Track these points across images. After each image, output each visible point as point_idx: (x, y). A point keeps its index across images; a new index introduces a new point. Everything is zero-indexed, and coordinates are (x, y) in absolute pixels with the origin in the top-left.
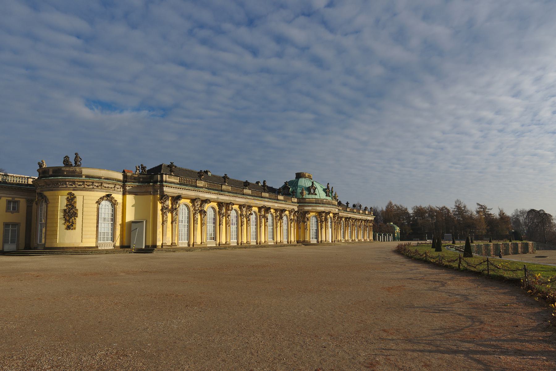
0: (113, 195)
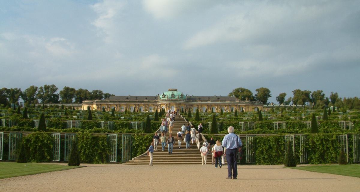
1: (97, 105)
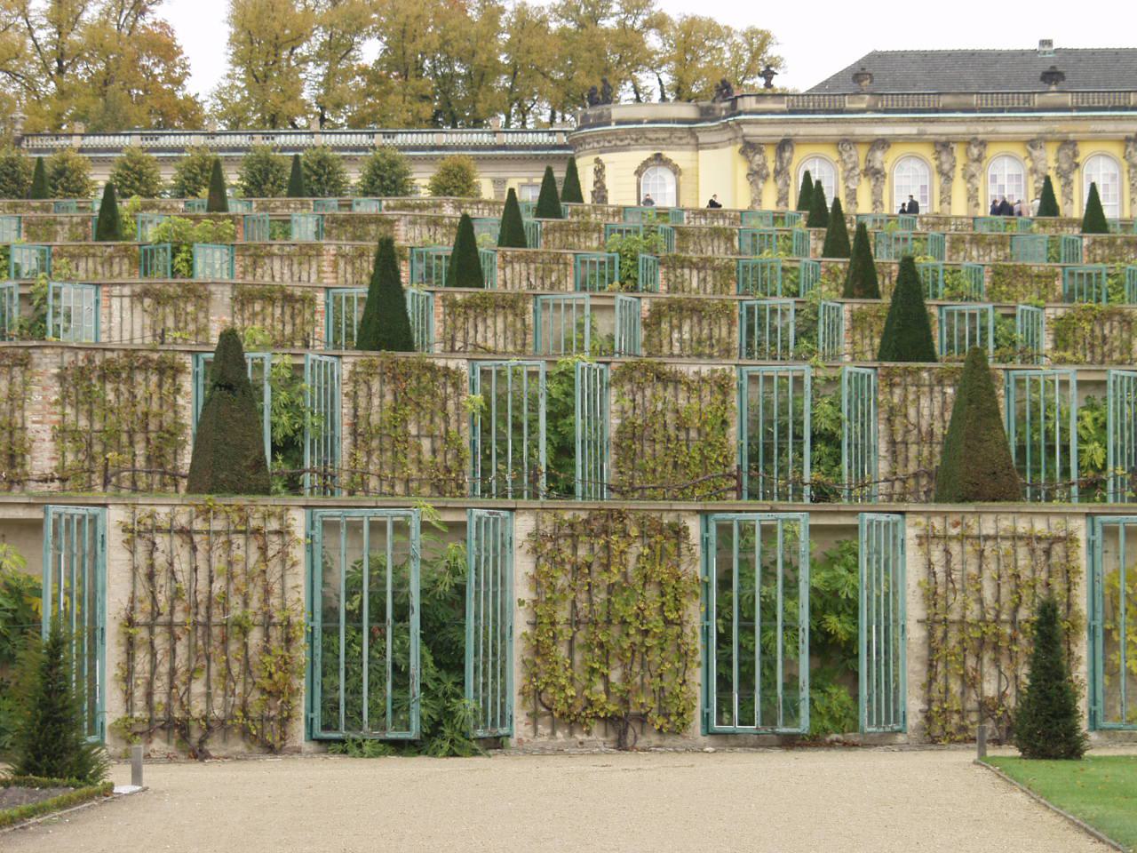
0: (667, 154)
1: (750, 148)
